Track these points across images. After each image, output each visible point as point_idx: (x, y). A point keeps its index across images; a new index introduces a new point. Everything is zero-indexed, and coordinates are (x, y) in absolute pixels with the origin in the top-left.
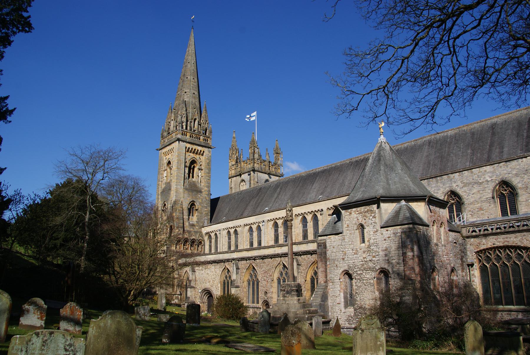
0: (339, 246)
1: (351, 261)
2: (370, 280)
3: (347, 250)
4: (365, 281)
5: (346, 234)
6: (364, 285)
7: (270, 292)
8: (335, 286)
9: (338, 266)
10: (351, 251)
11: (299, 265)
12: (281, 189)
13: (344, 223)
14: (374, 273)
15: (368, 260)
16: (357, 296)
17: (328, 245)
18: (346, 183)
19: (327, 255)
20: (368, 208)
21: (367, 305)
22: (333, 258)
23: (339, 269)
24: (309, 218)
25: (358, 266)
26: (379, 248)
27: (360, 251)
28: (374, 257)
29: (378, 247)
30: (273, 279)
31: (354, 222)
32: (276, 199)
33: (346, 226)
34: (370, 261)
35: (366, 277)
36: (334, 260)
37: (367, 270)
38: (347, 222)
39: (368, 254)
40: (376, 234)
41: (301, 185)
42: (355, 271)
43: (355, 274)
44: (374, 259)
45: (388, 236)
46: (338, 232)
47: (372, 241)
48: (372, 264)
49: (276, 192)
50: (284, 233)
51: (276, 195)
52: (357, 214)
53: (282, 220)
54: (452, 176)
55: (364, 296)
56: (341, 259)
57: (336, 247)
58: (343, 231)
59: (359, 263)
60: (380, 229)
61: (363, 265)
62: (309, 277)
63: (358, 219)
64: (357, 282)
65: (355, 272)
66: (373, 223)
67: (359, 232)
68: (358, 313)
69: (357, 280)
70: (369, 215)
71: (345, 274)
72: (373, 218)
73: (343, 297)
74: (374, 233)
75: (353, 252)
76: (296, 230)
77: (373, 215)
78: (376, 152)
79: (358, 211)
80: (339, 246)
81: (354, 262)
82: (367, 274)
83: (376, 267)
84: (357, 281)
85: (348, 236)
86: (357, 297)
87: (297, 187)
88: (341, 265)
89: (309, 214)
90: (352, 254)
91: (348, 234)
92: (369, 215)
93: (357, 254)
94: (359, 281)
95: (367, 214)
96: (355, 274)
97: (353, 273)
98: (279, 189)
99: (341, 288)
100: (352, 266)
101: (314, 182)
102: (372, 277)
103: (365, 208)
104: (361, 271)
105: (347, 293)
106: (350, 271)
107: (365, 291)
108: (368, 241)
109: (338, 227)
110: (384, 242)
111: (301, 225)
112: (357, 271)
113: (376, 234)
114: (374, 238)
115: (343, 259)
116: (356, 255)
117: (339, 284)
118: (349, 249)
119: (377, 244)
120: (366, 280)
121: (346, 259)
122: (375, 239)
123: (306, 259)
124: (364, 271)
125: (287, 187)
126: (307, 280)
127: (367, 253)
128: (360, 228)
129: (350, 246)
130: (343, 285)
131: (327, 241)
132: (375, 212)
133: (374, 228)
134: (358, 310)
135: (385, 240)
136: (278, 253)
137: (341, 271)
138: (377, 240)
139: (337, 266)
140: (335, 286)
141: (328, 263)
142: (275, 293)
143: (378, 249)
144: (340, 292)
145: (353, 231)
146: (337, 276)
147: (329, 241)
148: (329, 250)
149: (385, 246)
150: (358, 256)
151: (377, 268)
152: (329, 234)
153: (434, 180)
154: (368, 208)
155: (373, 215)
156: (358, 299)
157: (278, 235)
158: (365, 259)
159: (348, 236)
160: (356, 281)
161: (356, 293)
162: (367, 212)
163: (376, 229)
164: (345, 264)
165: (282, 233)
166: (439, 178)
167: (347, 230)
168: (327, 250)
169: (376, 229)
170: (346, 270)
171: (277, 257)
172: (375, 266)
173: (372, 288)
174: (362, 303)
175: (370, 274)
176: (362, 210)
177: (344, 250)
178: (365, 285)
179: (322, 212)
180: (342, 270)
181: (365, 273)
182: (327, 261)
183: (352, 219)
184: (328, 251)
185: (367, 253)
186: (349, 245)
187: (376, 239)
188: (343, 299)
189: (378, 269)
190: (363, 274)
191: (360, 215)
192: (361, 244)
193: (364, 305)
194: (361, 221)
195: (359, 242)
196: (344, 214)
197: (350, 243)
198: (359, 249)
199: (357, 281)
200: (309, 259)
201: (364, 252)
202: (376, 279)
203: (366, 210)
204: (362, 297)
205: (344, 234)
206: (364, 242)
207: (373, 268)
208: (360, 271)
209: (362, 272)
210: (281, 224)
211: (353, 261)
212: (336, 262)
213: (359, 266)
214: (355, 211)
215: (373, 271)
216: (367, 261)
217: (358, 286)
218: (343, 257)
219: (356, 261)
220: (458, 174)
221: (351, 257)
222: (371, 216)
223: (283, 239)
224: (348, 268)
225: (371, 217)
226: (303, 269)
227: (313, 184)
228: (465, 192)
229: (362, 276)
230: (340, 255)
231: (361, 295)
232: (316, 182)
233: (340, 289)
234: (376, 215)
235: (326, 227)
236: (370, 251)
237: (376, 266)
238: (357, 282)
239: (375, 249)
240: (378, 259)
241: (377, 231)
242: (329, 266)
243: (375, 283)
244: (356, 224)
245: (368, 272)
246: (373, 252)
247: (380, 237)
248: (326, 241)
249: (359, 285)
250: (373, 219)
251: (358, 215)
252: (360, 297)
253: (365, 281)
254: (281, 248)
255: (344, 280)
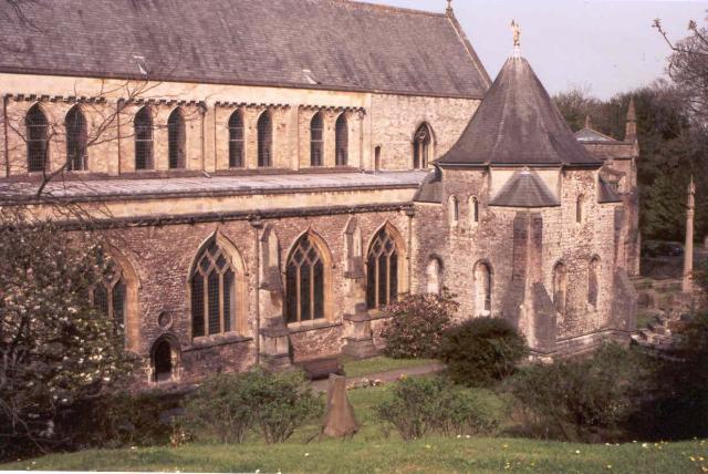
7: (180, 311)
24: (162, 116)
54: (427, 99)
61: (578, 251)
153: (406, 98)
166: (412, 98)
200: (291, 225)
206: (579, 220)
220: (433, 99)
228: (439, 128)
230: (555, 239)
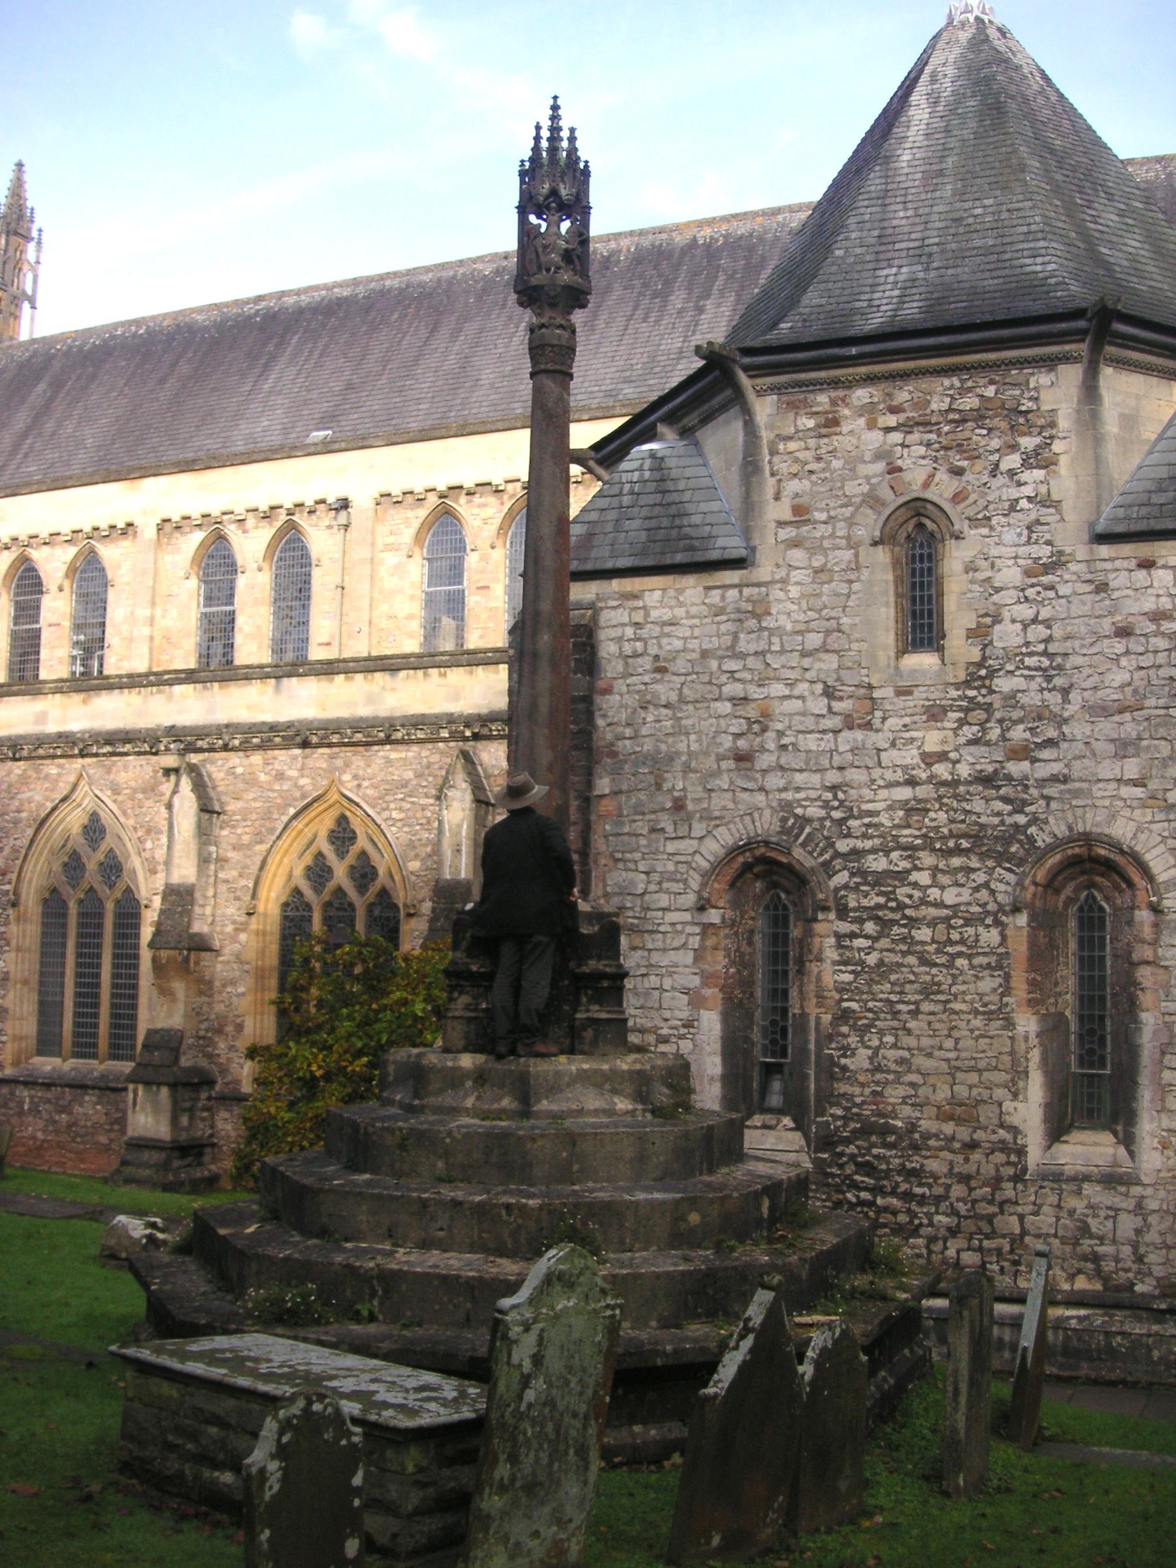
0: (714, 664)
1: (815, 779)
2: (968, 922)
3: (778, 689)
4: (923, 934)
5: (781, 574)
6: (912, 960)
8: (655, 958)
9: (690, 806)
10: (819, 705)
11: (212, 812)
12: (57, 385)
13: (770, 492)
14: (1011, 878)
15: (964, 771)
16: (853, 1040)
17: (607, 649)
18: (487, 377)
19: (600, 722)
20: (990, 391)
21: (931, 1111)
22: (648, 746)
23: (699, 829)
25: (871, 814)
26: (1065, 692)
27: (900, 702)
28: (1023, 752)
29: (1058, 681)
30: (16, 892)
31: (856, 489)
32: (24, 435)
33: (783, 511)
34: (986, 780)
35: (939, 905)
36: (659, 764)
37: (950, 853)
38: (793, 486)
39: (969, 732)
40: (1051, 587)
41: (184, 368)
42: (837, 854)
43: (842, 878)
44: (1017, 768)
45: (1149, 605)
46: (714, 555)
47: (1007, 636)
48: (998, 806)
49: (23, 401)
50: (78, 627)
51: (21, 420)
52: (888, 430)
53: (72, 551)
55: (911, 1042)
56: (720, 758)
57: (680, 665)
58: (753, 550)
59: (883, 794)
60: (1082, 552)
61: (914, 810)
62: (273, 895)
63: (893, 470)
64: (853, 935)
65: (838, 863)
66: (1024, 504)
67: (896, 563)
68: (850, 1169)
69: (861, 921)
70: (995, 443)
71: (747, 867)
72: (1026, 464)
73: (717, 1047)
74: (1028, 573)
75: (837, 706)
76: (158, 611)
77: (1028, 443)
78: (950, 71)
79: (894, 410)
80: (714, 664)
81: (834, 788)
82: (944, 880)
83: (1032, 830)
84: (855, 928)
85: (794, 592)
86: (846, 1050)
87: (162, 381)
88: (720, 802)
89: (251, 522)
90: (828, 723)
91: (796, 576)
92: (995, 443)
93: (868, 726)
94: (870, 927)
95: (978, 437)
96: (842, 878)
97: (826, 865)
98: (41, 387)
99: (707, 979)
100: (814, 811)
101: (273, 358)
102: (991, 907)
103: (963, 391)
104: (895, 855)
105: (749, 1016)
106: (798, 853)
107: (926, 1007)
108: (980, 634)
109: (696, 519)
110: (1119, 646)
111: (193, 583)
112: (856, 854)
113: (1051, 587)
114: (1027, 612)
115: (743, 758)
116: (859, 735)
117: (695, 942)
118: (802, 688)
119: (1050, 656)
120: (933, 923)
121: (764, 761)
122: (1035, 621)
123: (263, 777)
124: (927, 859)
125: (94, 377)
126: (261, 908)
127: (962, 723)
128: (902, 535)
129: (806, 663)
130: (720, 955)
131: (606, 617)
132: (1052, 425)
133: (1028, 542)
134: (848, 1141)
135: (1124, 632)
136: (60, 735)
137: (713, 848)
138: (1057, 631)
139: (679, 805)
140: (655, 958)
141: (603, 785)
142: (25, 982)
143: (1054, 699)
144: (696, 1001)
145: (848, 555)
146: (676, 887)
147: (622, 616)
148: (620, 686)
149: (1119, 677)
150: (881, 740)
151: (1042, 839)
152: (624, 562)
154: (990, 391)
155: (1028, 443)
156: (860, 1060)
157: (36, 635)
158: (942, 770)
159: (794, 592)
160: (845, 927)
161: (844, 1016)
162: (978, 417)
163: (1046, 551)
164: (760, 798)
165: (67, 624)
167: (795, 544)
168: (601, 684)
169: (1046, 551)
170: (767, 843)
171: (54, 757)
172: (1022, 819)
173: (988, 984)
174: (894, 1094)
175: (981, 878)
176: (938, 404)
177: (755, 692)
178: (924, 961)
179: (343, 514)
180: (726, 837)
181: (935, 870)
182: (598, 769)
183: (836, 464)
184: (608, 691)
185: (962, 723)
186: (804, 654)
187: (1048, 624)
188: (718, 1060)
189: (1050, 849)
190: (915, 876)
191: (915, 437)
192: (901, 652)
193: (907, 1111)
194: (926, 485)
195: (888, 639)
196: (771, 427)
197: (814, 640)
198: (889, 692)
199: (855, 928)
200: (280, 776)
201: (935, 714)
202: (1022, 919)
203: (969, 402)
204: (895, 1046)
205: (764, 571)
207: (1007, 840)
208: (887, 853)
209: (905, 865)
210: (61, 574)
211: (833, 777)
212: (676, 782)
213: (884, 819)
214: (869, 411)
215: (1002, 858)
216: (955, 783)
217: (862, 963)
218: (742, 743)
219: (853, 775)
221: (811, 742)
222: (1014, 447)
223: (67, 660)
224: (785, 831)
225: (1012, 461)
226: (233, 839)
227: (267, 368)
229: (902, 892)
231: (881, 1033)
232: (284, 359)
233: (696, 981)
234: (1057, 446)
235: (594, 516)
236: (988, 708)
237: (1034, 820)
238: (853, 935)
239: (1032, 699)
240: (1056, 768)
241: (1057, 563)
242: (606, 806)
243: (1019, 947)
244: (872, 500)
245: (956, 862)
246: (1016, 714)
247: (1086, 609)
248: (595, 619)
249: (872, 959)
250: (1026, 476)
251: (897, 437)
252: (876, 1050)
253: (923, 934)
254: (85, 702)
255: (729, 914)
